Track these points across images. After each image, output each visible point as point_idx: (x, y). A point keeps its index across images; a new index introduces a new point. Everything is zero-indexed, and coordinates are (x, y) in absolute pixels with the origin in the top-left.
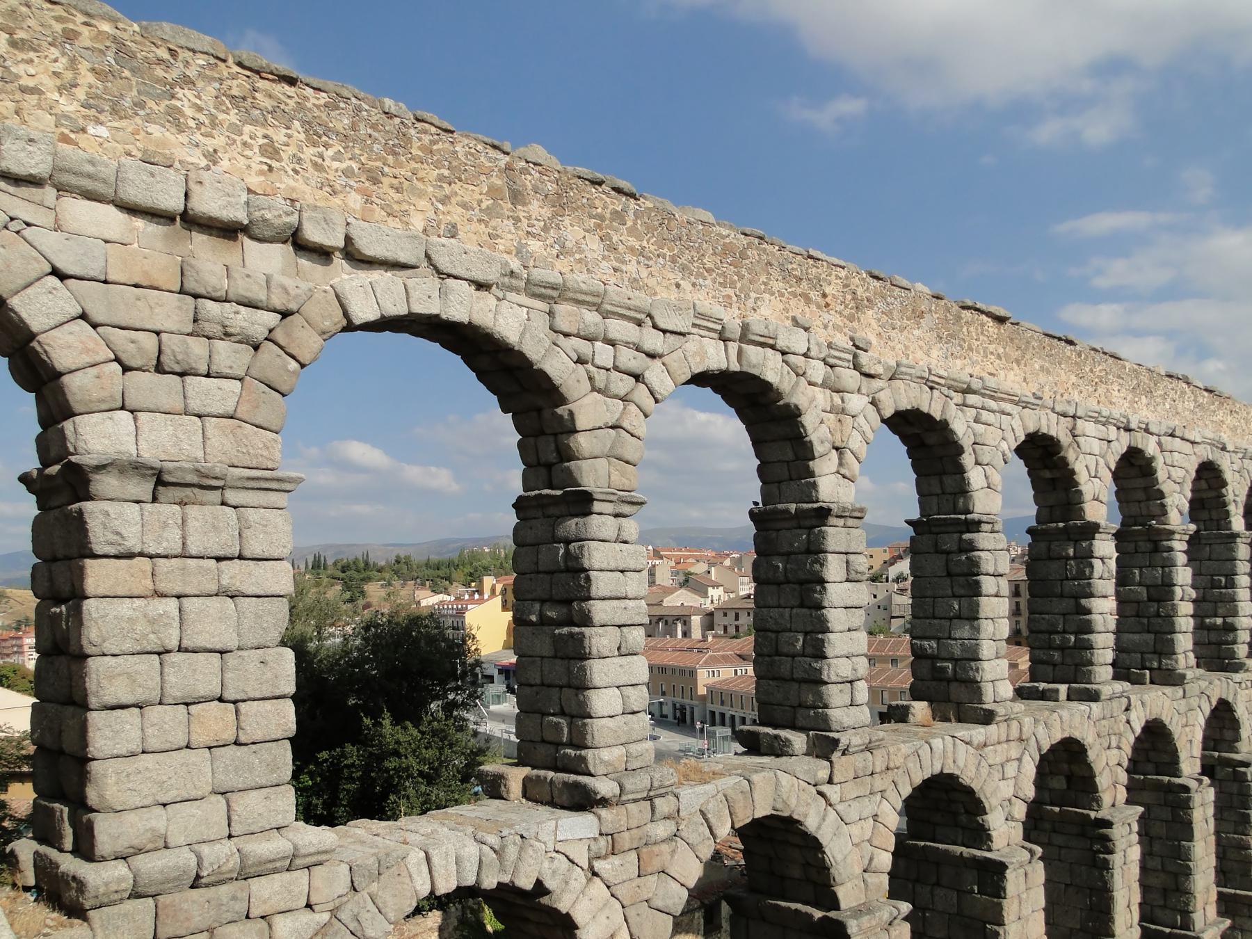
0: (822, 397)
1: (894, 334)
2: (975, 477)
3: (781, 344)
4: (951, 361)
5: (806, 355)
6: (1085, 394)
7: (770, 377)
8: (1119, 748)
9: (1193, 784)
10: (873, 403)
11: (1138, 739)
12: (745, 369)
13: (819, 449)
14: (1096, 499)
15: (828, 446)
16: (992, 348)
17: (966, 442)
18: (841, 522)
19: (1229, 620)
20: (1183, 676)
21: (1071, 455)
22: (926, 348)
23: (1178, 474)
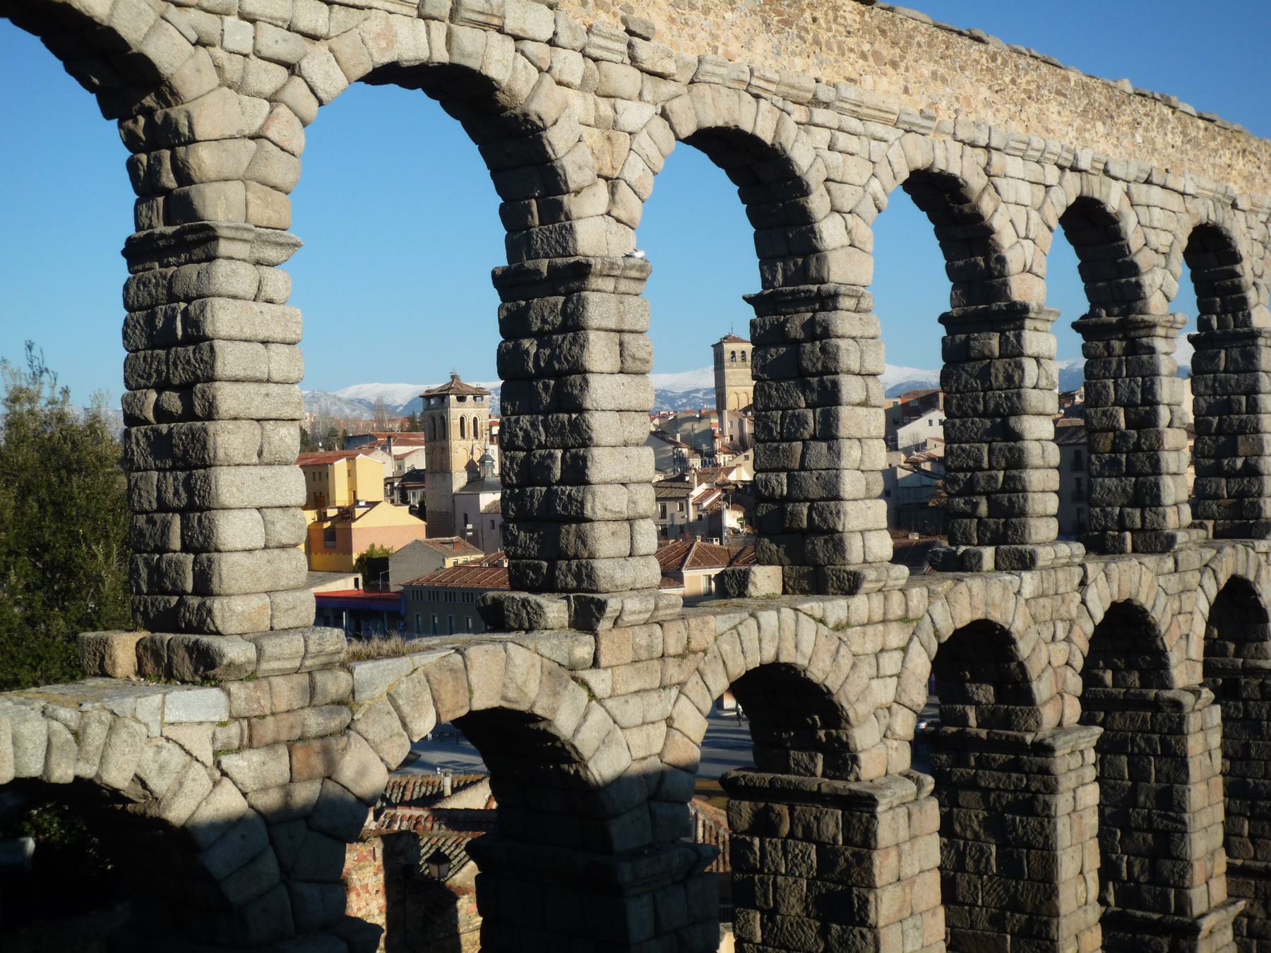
0: (580, 105)
1: (694, 16)
2: (830, 232)
3: (510, 26)
4: (785, 60)
5: (551, 43)
6: (1004, 115)
7: (495, 71)
8: (1068, 639)
9: (1188, 699)
10: (664, 115)
11: (1098, 628)
12: (457, 60)
13: (574, 177)
14: (1028, 270)
15: (587, 176)
16: (851, 42)
17: (814, 179)
18: (609, 284)
19: (1252, 461)
20: (1171, 539)
21: (986, 206)
22: (744, 38)
23: (1161, 240)
